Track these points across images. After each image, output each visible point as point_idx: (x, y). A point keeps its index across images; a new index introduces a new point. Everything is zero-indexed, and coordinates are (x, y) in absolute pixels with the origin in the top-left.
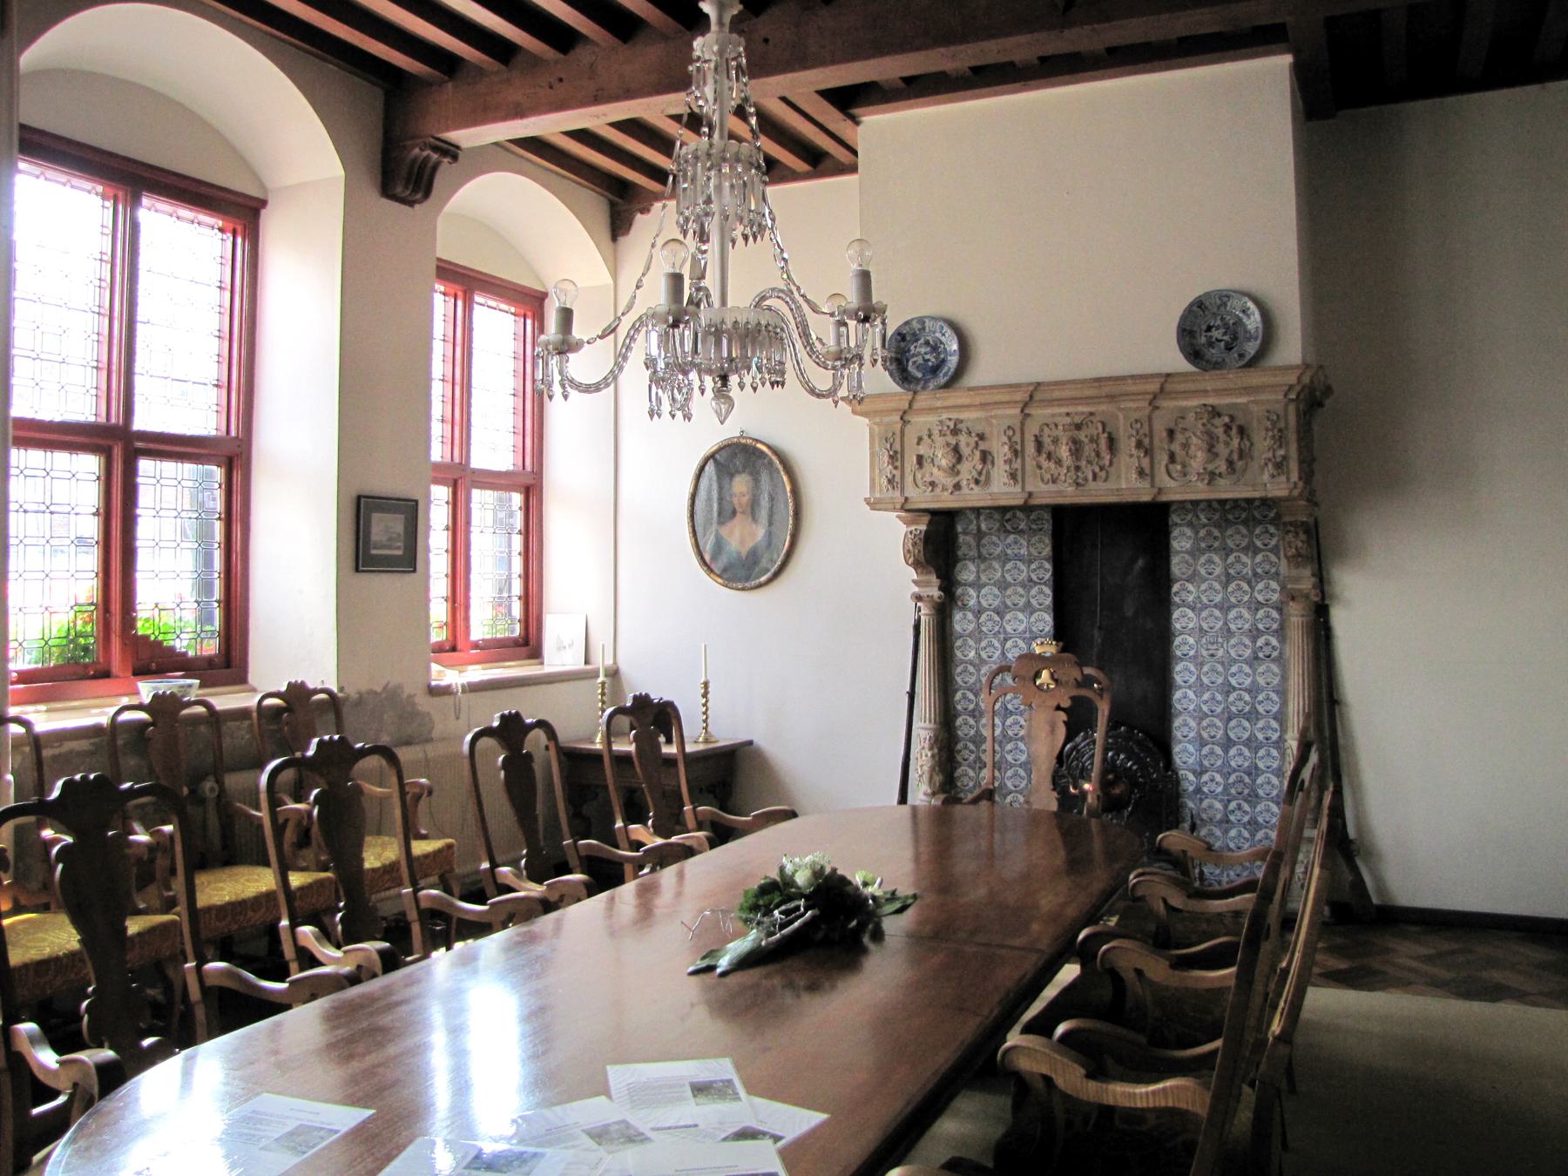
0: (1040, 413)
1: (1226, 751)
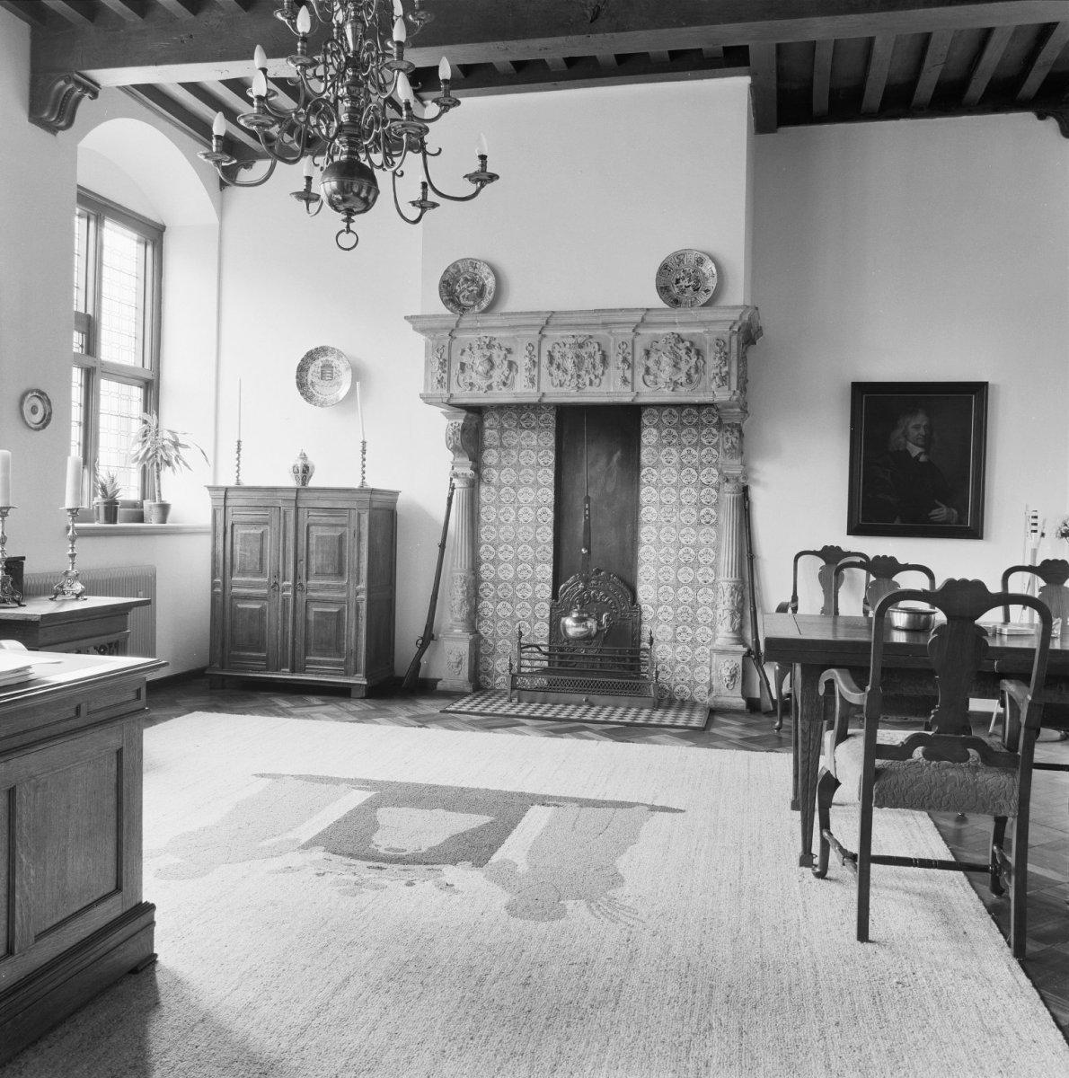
0: (554, 335)
1: (676, 591)
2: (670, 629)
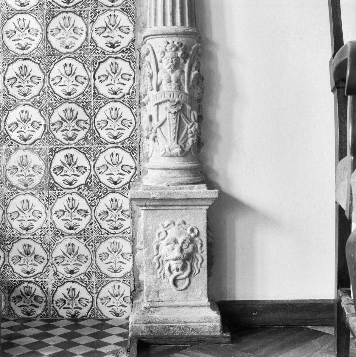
1: (47, 72)
2: (36, 160)
